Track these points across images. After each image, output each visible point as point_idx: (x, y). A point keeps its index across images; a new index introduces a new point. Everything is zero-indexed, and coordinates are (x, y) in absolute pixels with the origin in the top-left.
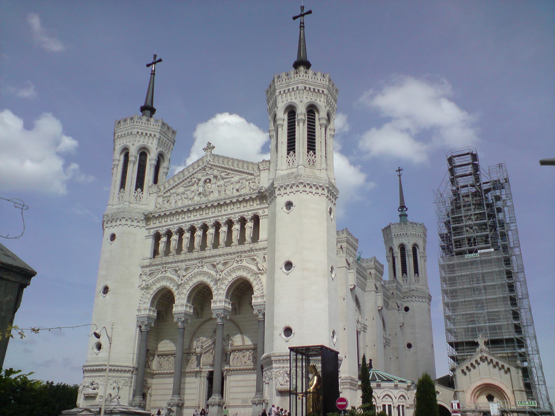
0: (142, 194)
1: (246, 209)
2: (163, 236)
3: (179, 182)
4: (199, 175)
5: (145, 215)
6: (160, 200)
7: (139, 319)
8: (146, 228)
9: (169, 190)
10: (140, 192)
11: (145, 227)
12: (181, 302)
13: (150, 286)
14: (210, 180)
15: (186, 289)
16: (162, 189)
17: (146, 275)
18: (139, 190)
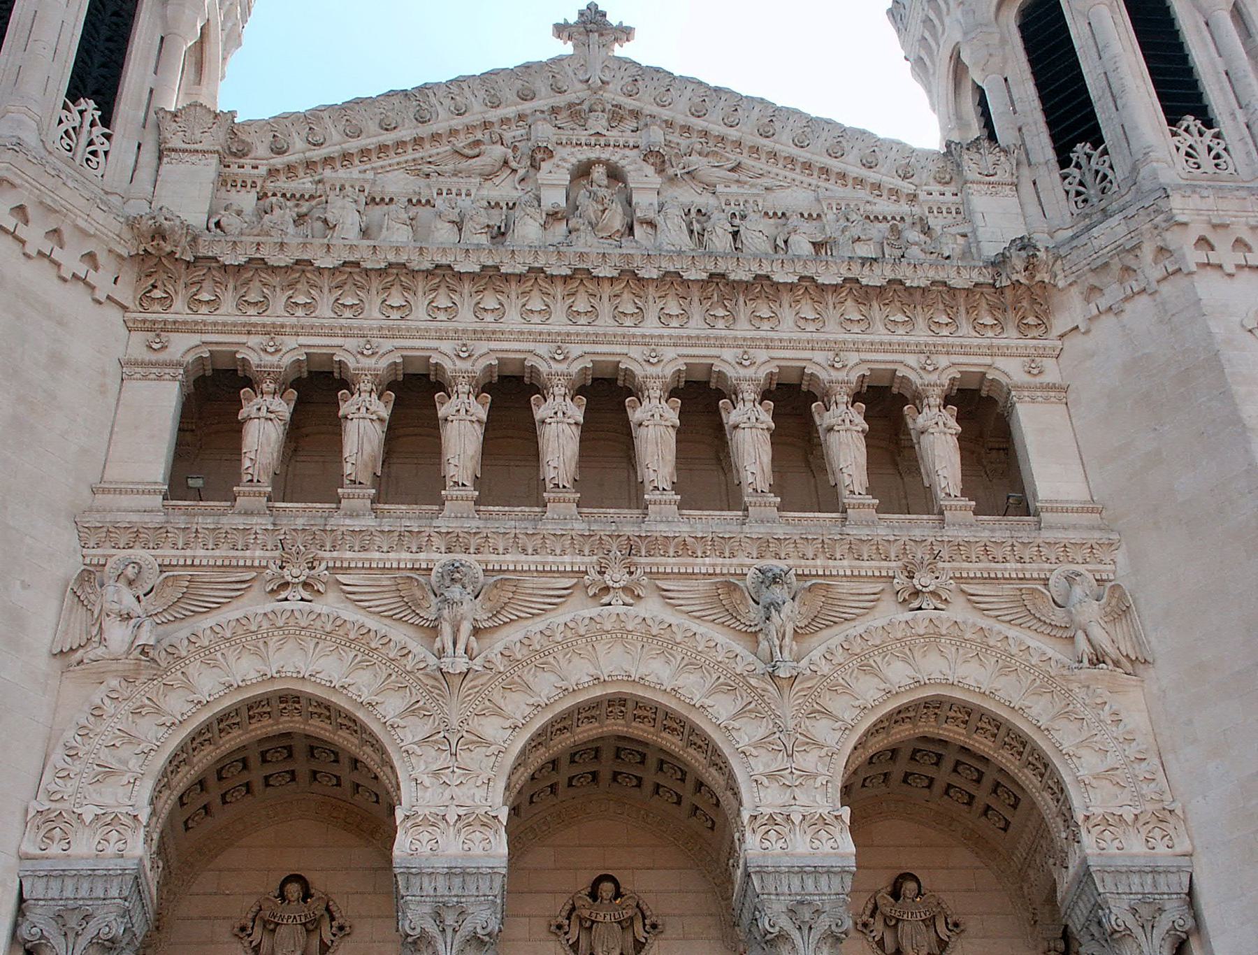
0: (108, 137)
1: (900, 336)
2: (268, 386)
3: (389, 138)
4: (544, 132)
5: (159, 234)
6: (247, 200)
7: (34, 890)
8: (127, 314)
9: (309, 165)
10: (92, 124)
11: (125, 308)
12: (469, 803)
13: (164, 664)
14: (615, 174)
15: (498, 712)
16: (261, 150)
17: (130, 583)
18: (89, 106)
